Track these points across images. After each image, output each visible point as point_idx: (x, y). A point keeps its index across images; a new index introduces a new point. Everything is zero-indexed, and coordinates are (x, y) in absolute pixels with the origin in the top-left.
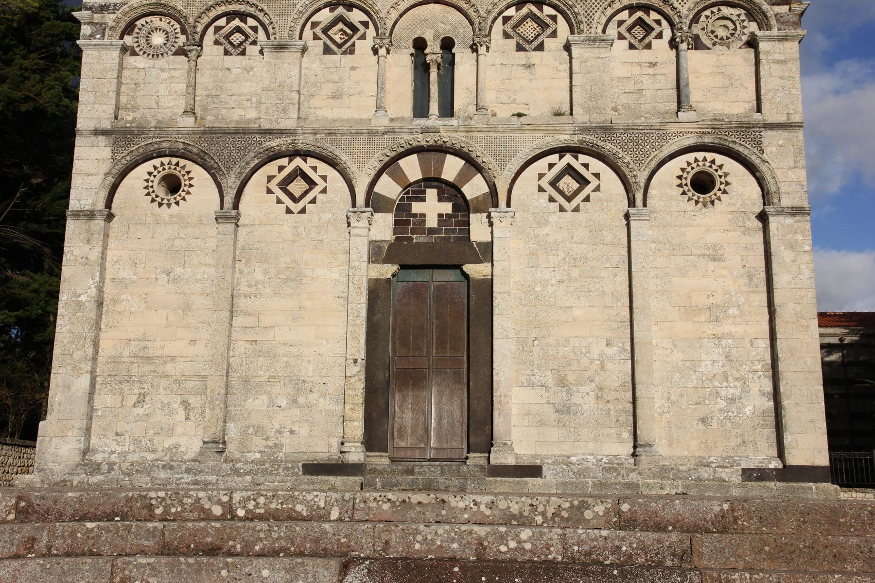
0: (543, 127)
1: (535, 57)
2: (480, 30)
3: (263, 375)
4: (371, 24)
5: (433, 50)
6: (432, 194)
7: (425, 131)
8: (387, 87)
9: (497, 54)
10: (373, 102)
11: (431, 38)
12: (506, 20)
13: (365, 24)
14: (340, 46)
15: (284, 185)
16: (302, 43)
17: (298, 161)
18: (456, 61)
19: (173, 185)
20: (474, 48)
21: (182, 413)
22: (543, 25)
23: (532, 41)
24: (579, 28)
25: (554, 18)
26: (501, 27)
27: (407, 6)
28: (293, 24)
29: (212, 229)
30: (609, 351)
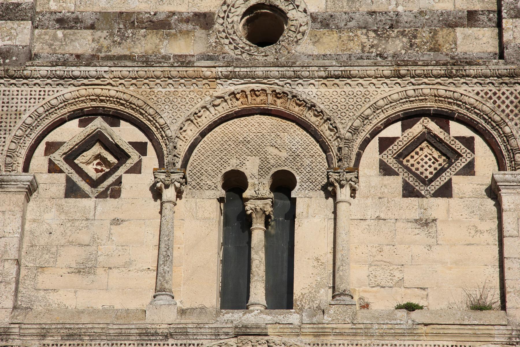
0: (453, 329)
1: (437, 207)
2: (340, 160)
4: (150, 148)
5: (258, 193)
7: (242, 332)
8: (176, 253)
9: (369, 201)
10: (150, 280)
11: (255, 171)
12: (385, 144)
13: (141, 148)
14: (94, 184)
16: (27, 177)
18: (298, 211)
20: (329, 191)
22: (450, 155)
23: (431, 181)
24: (513, 159)
25: (469, 143)
26: (377, 156)
27: (215, 118)
28: (13, 146)
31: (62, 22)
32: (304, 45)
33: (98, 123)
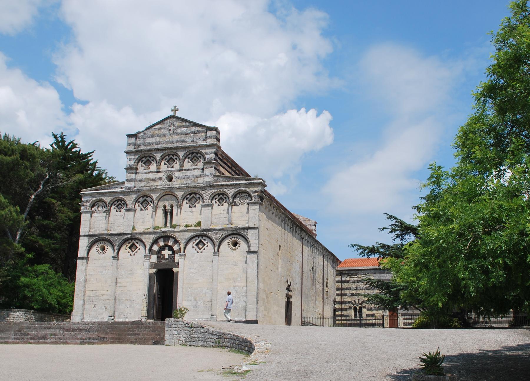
15: (130, 248)
17: (133, 241)
19: (103, 249)
21: (105, 309)
25: (199, 198)
29: (111, 260)
30: (207, 291)
31: (139, 180)
33: (145, 198)
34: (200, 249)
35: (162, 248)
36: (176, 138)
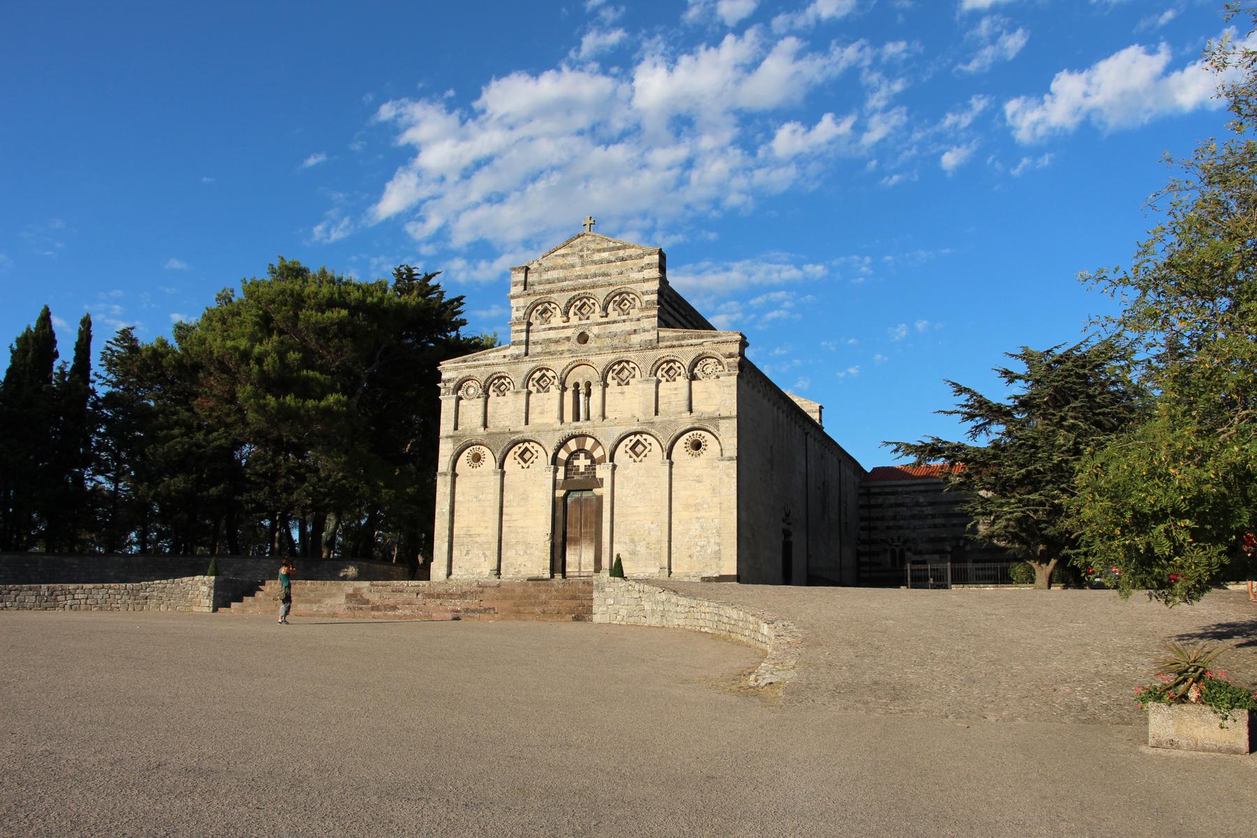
3: (514, 541)
5: (582, 389)
6: (582, 455)
15: (521, 455)
32: (591, 344)
34: (638, 456)
35: (574, 455)
36: (593, 269)
